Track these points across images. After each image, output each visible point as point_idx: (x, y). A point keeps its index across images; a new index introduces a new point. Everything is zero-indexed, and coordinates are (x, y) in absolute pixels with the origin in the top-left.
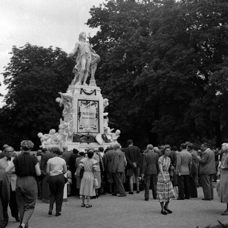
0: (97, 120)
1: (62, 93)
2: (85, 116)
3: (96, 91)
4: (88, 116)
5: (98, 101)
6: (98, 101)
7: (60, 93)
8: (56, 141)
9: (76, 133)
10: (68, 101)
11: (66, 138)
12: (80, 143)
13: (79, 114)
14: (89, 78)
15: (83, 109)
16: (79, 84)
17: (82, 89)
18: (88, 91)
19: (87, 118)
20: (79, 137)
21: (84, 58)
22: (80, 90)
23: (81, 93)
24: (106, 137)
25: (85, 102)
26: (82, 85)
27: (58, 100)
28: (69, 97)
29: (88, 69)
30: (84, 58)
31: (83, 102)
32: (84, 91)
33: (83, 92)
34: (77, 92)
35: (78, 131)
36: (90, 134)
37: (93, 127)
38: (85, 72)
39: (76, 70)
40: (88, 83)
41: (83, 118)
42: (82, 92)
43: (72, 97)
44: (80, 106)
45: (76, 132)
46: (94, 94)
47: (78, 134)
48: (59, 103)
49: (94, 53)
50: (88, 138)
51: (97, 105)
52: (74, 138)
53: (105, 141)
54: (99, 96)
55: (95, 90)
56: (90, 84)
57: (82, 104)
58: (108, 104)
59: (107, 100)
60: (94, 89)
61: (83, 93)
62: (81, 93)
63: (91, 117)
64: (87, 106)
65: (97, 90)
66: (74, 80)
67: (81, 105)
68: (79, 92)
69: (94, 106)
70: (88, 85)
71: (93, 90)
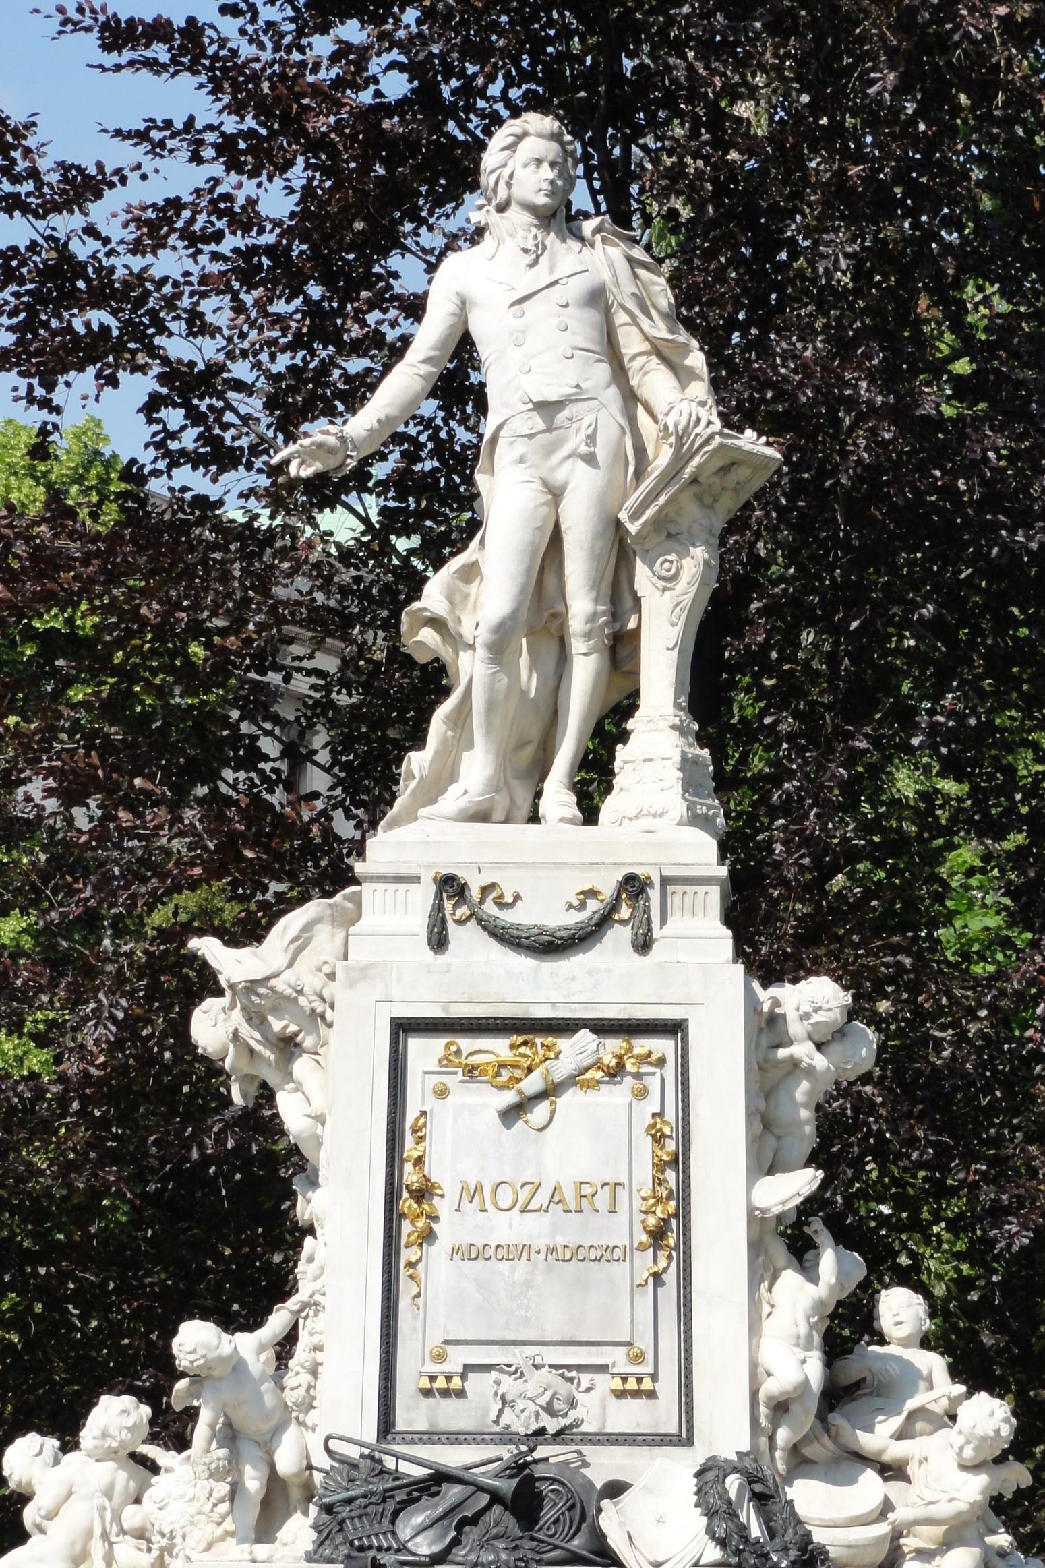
0: (671, 1278)
1: (227, 944)
2: (506, 1228)
3: (654, 894)
4: (535, 1230)
6: (674, 1028)
7: (208, 947)
9: (353, 1452)
13: (405, 1200)
15: (461, 1128)
16: (481, 816)
17: (450, 886)
18: (546, 910)
19: (511, 1253)
20: (386, 1496)
21: (522, 473)
22: (423, 896)
23: (439, 941)
25: (499, 1047)
26: (534, 818)
27: (211, 1027)
28: (283, 1003)
31: (466, 1044)
32: (490, 908)
33: (472, 923)
35: (401, 1424)
36: (537, 1455)
37: (603, 1369)
39: (436, 623)
40: (594, 780)
42: (451, 925)
44: (431, 1104)
45: (371, 1436)
46: (619, 936)
47: (390, 1462)
48: (213, 1069)
49: (682, 375)
52: (328, 1509)
53: (722, 1543)
55: (633, 886)
56: (609, 808)
57: (453, 1080)
61: (466, 939)
62: (439, 941)
63: (571, 1230)
64: (509, 1097)
65: (666, 881)
66: (417, 762)
67: (442, 1093)
70: (590, 815)
71: (608, 889)
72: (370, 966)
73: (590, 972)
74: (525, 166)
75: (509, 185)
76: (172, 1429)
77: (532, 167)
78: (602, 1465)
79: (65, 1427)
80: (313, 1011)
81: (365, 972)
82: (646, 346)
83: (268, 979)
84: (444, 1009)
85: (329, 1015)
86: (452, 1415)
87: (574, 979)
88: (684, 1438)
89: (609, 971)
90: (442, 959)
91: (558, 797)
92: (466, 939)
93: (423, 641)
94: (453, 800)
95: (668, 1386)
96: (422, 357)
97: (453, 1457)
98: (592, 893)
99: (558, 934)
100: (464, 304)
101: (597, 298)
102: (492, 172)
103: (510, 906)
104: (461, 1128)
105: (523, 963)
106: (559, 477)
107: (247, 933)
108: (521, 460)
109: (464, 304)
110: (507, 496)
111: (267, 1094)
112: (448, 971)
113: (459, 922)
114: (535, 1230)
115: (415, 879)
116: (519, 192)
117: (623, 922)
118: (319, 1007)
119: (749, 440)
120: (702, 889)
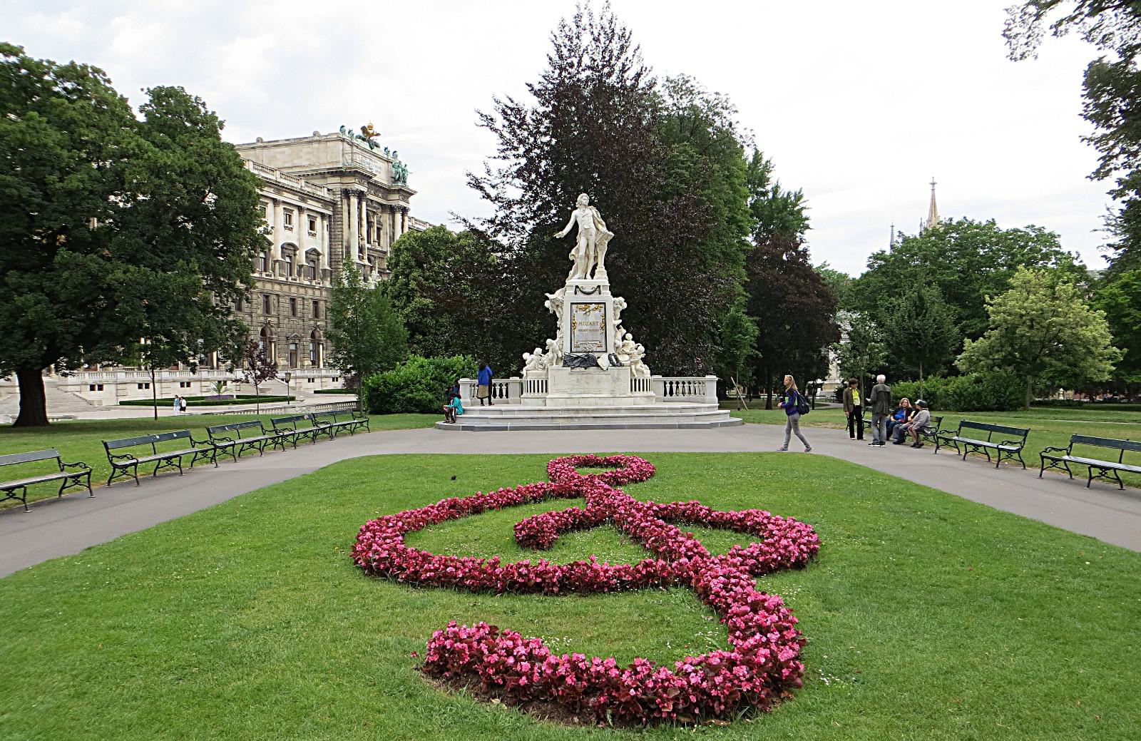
2: (584, 328)
4: (588, 327)
5: (604, 303)
6: (604, 303)
7: (547, 294)
8: (541, 365)
10: (558, 306)
11: (555, 361)
12: (572, 368)
13: (573, 325)
14: (595, 267)
15: (579, 317)
17: (577, 287)
23: (576, 293)
24: (617, 359)
27: (547, 304)
29: (592, 253)
34: (570, 291)
38: (587, 256)
40: (592, 275)
41: (580, 330)
48: (548, 310)
50: (585, 360)
51: (603, 310)
54: (607, 293)
55: (599, 286)
58: (625, 305)
59: (621, 299)
61: (579, 293)
62: (576, 293)
66: (571, 272)
68: (573, 292)
69: (597, 312)
76: (545, 352)
78: (596, 355)
79: (531, 353)
86: (579, 349)
88: (606, 352)
91: (588, 276)
92: (579, 293)
93: (571, 258)
94: (576, 276)
95: (604, 346)
97: (579, 354)
100: (576, 217)
101: (593, 216)
104: (579, 317)
105: (586, 296)
107: (552, 293)
110: (582, 241)
111: (554, 312)
114: (588, 327)
119: (611, 233)
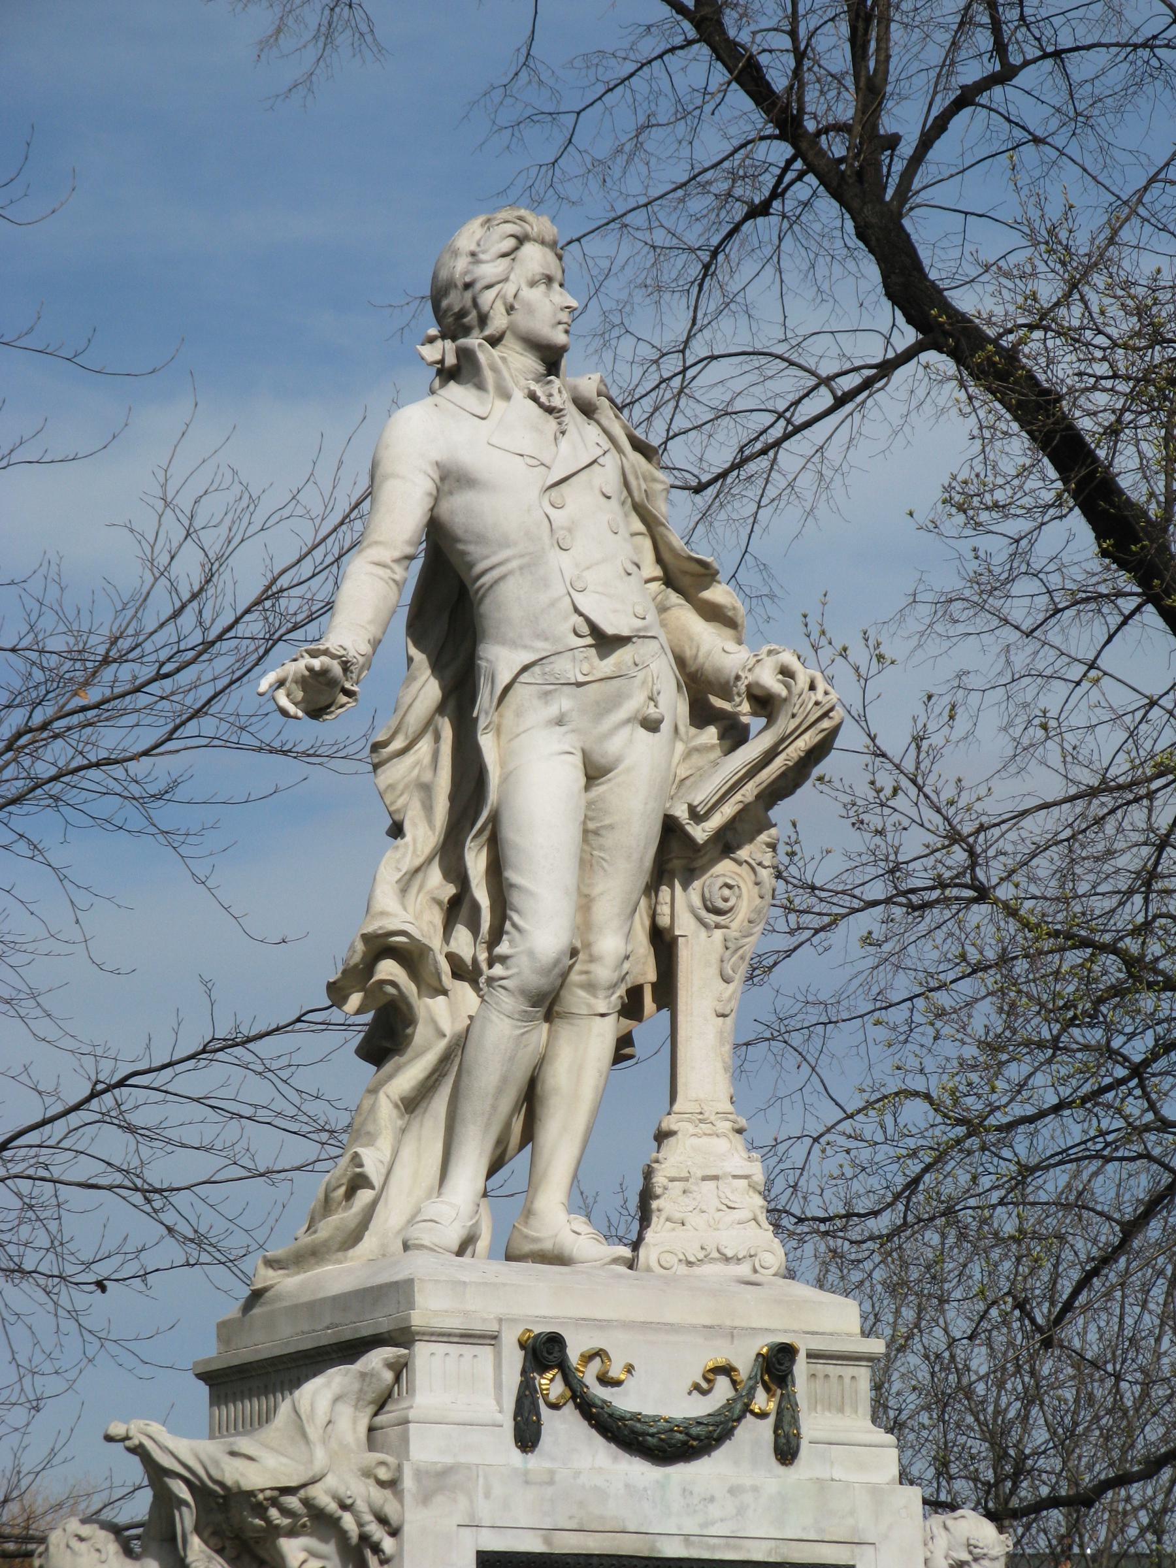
17: (544, 1352)
23: (527, 1436)
30: (560, 721)
42: (544, 1410)
43: (383, 1520)
60: (761, 1344)
62: (527, 1436)
71: (744, 1365)
72: (445, 1472)
73: (733, 1491)
74: (533, 284)
75: (510, 309)
77: (543, 287)
80: (364, 1538)
81: (440, 1480)
82: (658, 572)
83: (304, 1486)
84: (547, 1541)
85: (388, 1544)
87: (712, 1499)
89: (755, 1489)
90: (533, 1461)
96: (397, 554)
98: (726, 1370)
99: (695, 1431)
100: (451, 479)
102: (489, 287)
103: (618, 1383)
106: (614, 746)
108: (560, 721)
109: (451, 479)
112: (551, 1482)
113: (554, 1406)
115: (491, 1339)
116: (522, 320)
117: (763, 1415)
118: (376, 1531)
120: (848, 1371)
